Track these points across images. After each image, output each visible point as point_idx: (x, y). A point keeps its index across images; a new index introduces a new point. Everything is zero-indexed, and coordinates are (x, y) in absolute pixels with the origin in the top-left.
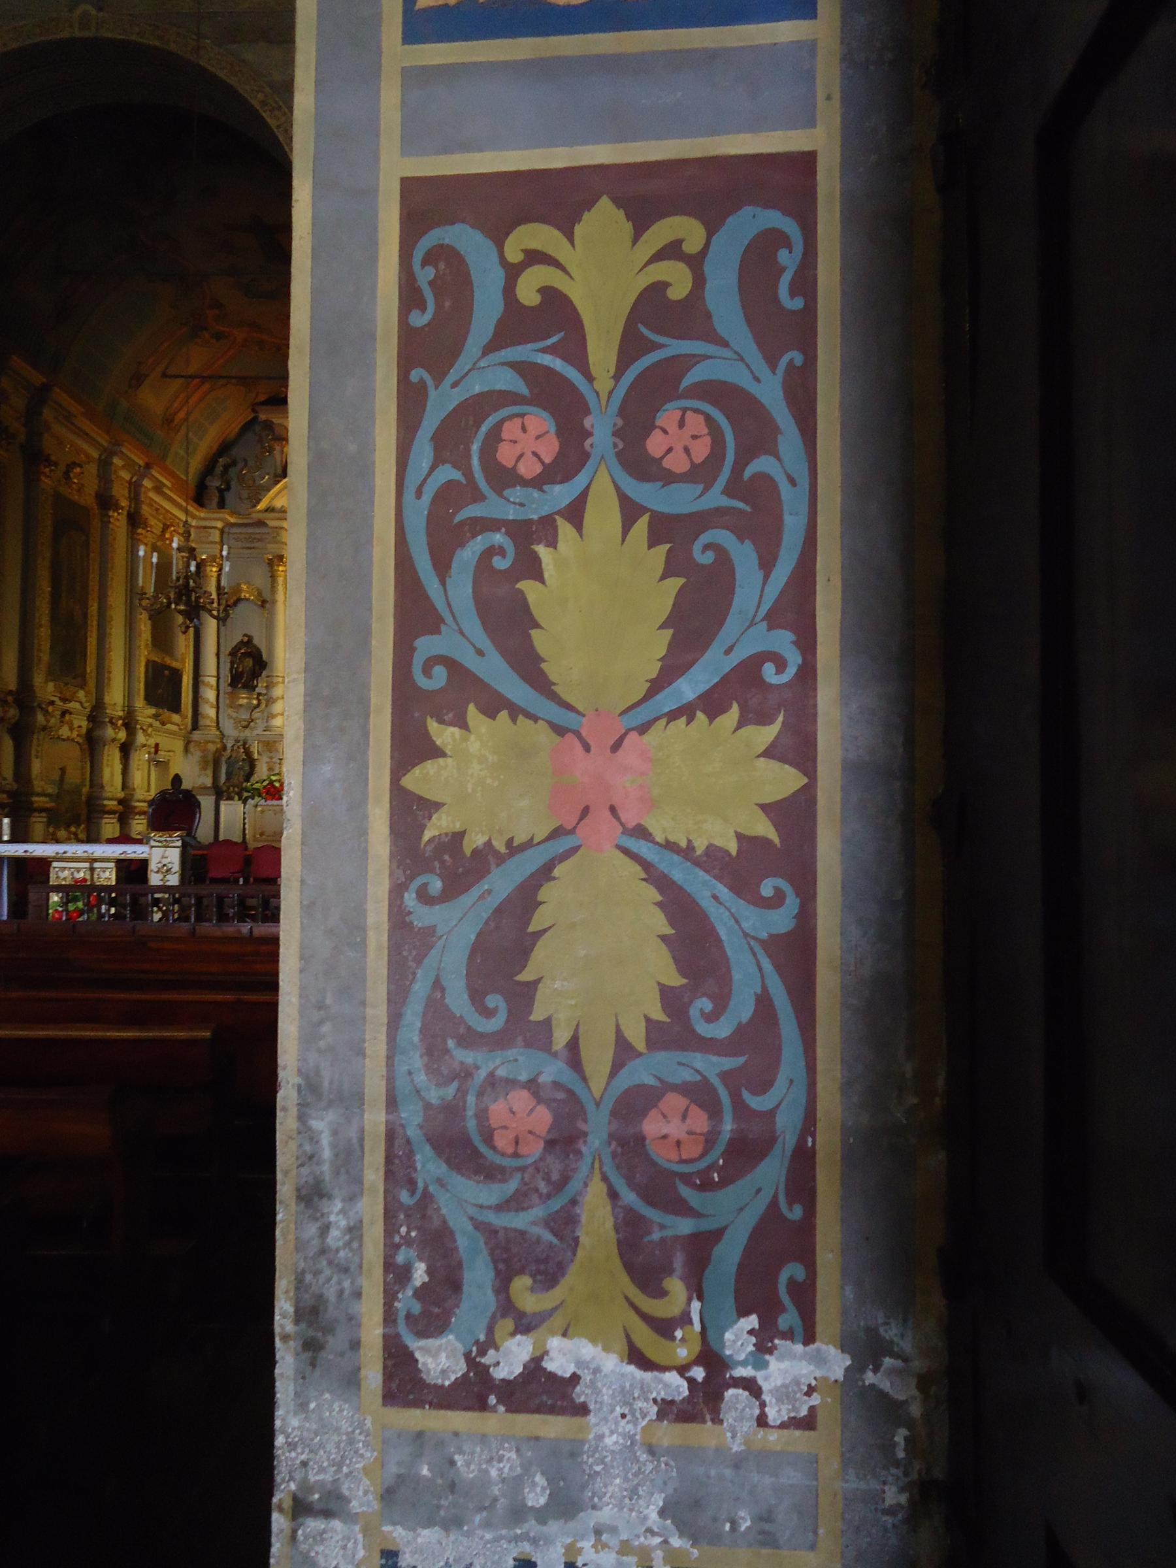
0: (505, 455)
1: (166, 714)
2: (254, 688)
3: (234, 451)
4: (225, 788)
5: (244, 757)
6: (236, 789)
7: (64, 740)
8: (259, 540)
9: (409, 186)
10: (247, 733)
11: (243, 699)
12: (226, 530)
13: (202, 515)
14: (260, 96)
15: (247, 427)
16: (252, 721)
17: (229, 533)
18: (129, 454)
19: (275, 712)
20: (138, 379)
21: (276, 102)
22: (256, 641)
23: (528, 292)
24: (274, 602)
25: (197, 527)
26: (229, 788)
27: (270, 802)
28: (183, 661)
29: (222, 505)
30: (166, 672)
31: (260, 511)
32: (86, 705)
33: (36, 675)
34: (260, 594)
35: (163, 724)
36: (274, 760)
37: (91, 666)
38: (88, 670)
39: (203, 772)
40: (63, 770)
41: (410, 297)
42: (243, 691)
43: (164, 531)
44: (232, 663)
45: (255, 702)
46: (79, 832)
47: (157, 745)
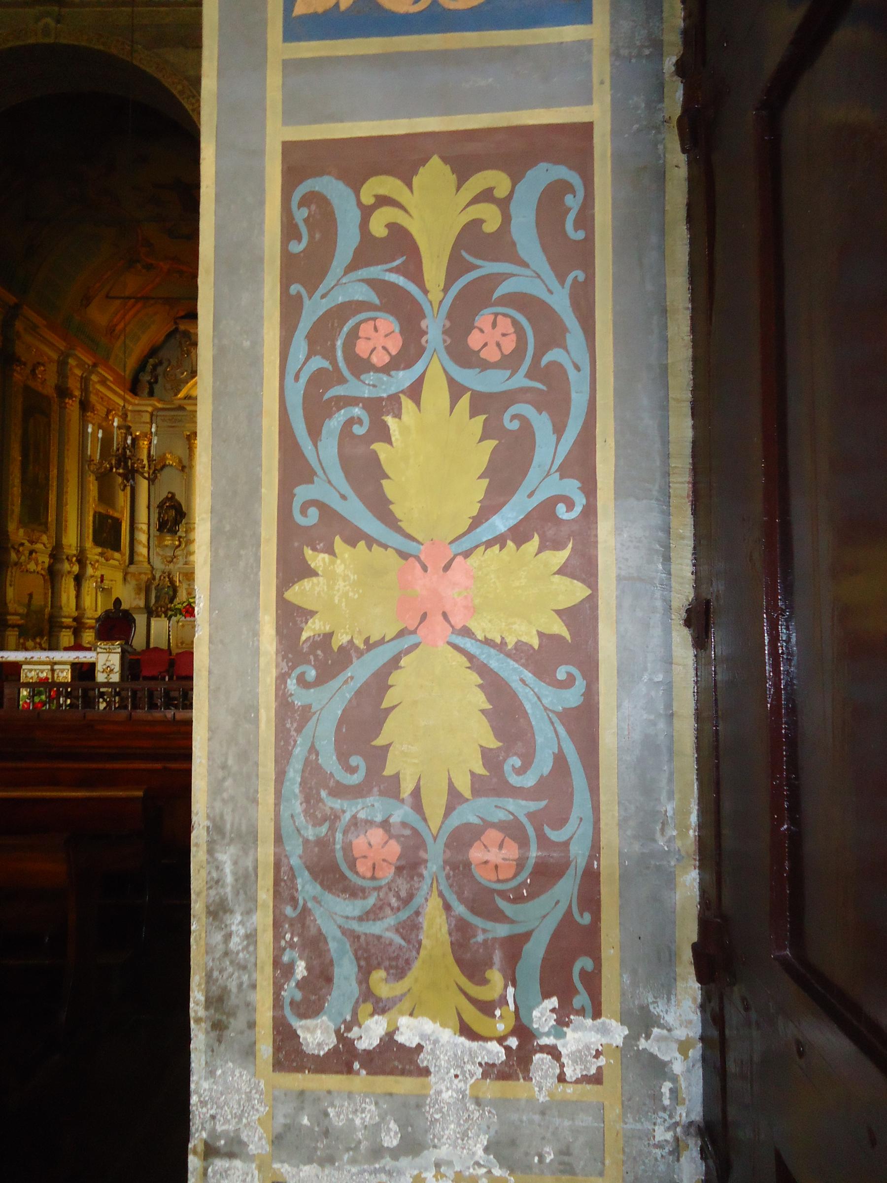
0: (362, 348)
1: (110, 552)
2: (176, 532)
4: (154, 608)
6: (163, 609)
7: (31, 572)
8: (180, 421)
9: (289, 148)
10: (171, 565)
11: (168, 540)
13: (137, 402)
14: (180, 87)
15: (170, 335)
16: (175, 557)
18: (80, 355)
20: (87, 300)
21: (191, 91)
22: (177, 497)
23: (378, 227)
25: (132, 411)
26: (157, 608)
29: (151, 394)
30: (110, 521)
31: (180, 399)
32: (48, 546)
33: (9, 523)
34: (180, 461)
35: (107, 560)
37: (52, 517)
38: (50, 519)
40: (31, 595)
41: (290, 231)
42: (169, 534)
43: (107, 415)
44: (160, 514)
45: (177, 543)
46: (42, 642)
47: (102, 576)
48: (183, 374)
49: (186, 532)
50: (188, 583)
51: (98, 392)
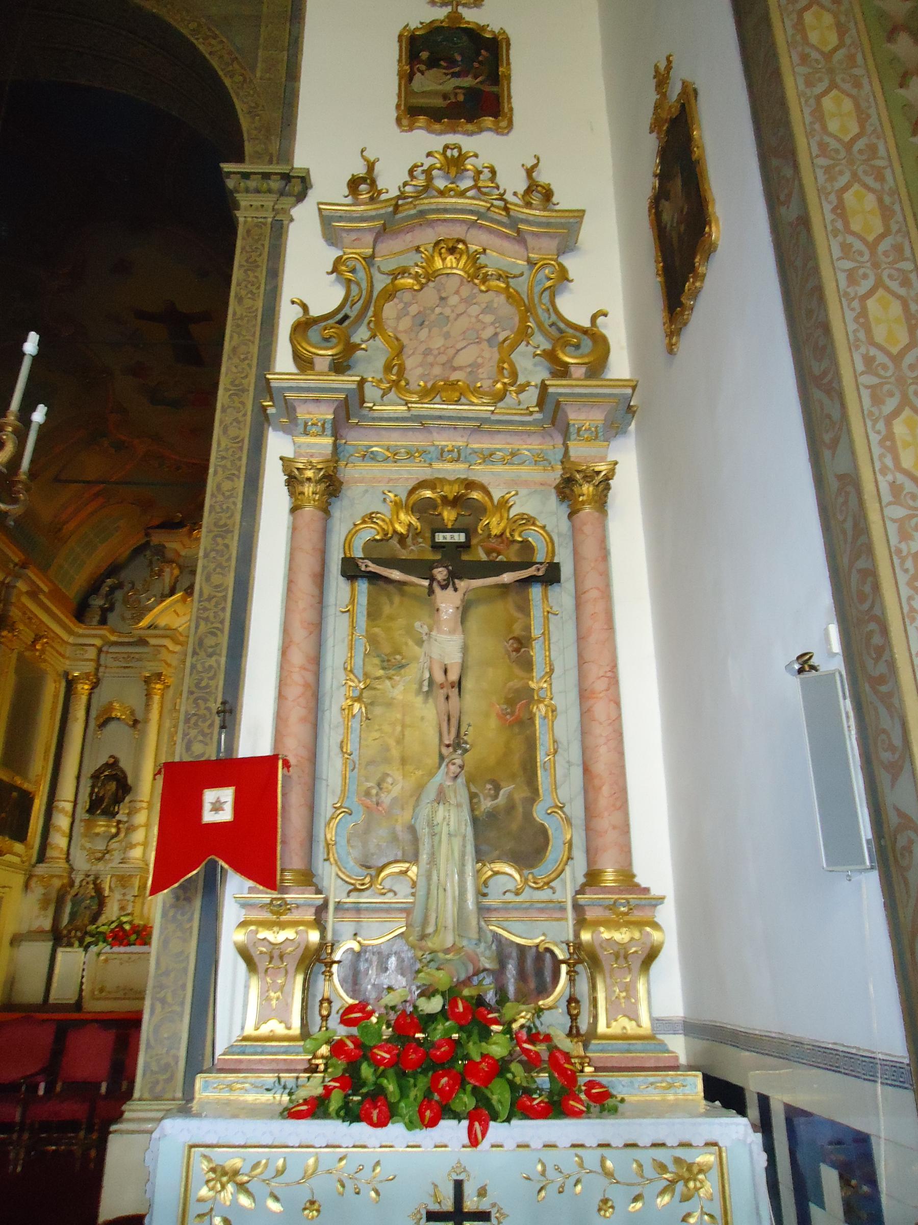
2: (114, 815)
3: (125, 575)
4: (65, 932)
5: (94, 894)
6: (79, 934)
8: (138, 660)
10: (100, 866)
11: (102, 826)
12: (105, 649)
13: (81, 631)
14: (193, 25)
15: (138, 551)
17: (107, 652)
19: (134, 842)
21: (209, 29)
22: (123, 764)
24: (147, 721)
26: (70, 932)
27: (116, 949)
28: (37, 783)
29: (103, 622)
34: (133, 713)
36: (127, 897)
39: (43, 912)
42: (103, 818)
43: (34, 642)
44: (93, 787)
45: (114, 830)
48: (149, 599)
49: (129, 814)
50: (123, 891)
51: (24, 610)
